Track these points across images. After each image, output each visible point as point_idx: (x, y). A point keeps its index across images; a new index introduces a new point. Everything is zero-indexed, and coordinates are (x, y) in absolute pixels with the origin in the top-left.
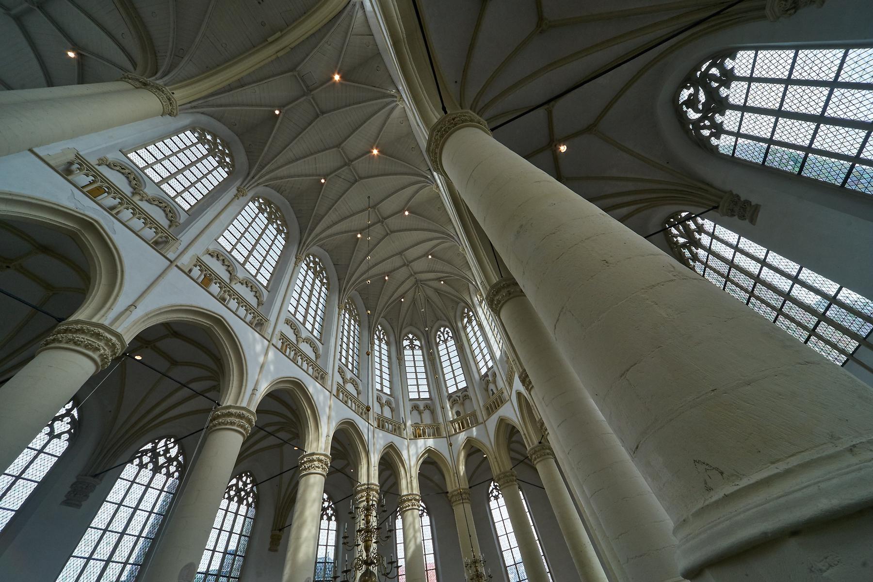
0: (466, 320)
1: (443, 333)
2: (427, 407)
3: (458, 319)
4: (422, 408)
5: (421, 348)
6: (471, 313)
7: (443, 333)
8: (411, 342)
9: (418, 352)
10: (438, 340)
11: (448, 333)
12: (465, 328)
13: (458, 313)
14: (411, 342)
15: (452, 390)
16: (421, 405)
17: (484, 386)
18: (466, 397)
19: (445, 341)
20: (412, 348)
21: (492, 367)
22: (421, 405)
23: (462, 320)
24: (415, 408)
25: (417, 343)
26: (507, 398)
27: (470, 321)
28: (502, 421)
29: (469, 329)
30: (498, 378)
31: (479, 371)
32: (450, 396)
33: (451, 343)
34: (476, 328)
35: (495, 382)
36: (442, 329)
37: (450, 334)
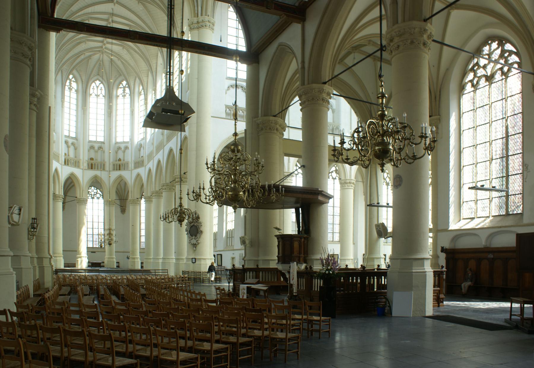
0: (120, 91)
1: (97, 87)
4: (70, 144)
5: (77, 91)
7: (97, 87)
8: (70, 83)
9: (74, 95)
10: (91, 91)
11: (101, 89)
13: (117, 82)
14: (70, 83)
17: (116, 149)
20: (70, 89)
22: (70, 141)
23: (118, 88)
25: (74, 85)
27: (124, 96)
29: (120, 100)
32: (90, 142)
33: (102, 101)
36: (98, 82)
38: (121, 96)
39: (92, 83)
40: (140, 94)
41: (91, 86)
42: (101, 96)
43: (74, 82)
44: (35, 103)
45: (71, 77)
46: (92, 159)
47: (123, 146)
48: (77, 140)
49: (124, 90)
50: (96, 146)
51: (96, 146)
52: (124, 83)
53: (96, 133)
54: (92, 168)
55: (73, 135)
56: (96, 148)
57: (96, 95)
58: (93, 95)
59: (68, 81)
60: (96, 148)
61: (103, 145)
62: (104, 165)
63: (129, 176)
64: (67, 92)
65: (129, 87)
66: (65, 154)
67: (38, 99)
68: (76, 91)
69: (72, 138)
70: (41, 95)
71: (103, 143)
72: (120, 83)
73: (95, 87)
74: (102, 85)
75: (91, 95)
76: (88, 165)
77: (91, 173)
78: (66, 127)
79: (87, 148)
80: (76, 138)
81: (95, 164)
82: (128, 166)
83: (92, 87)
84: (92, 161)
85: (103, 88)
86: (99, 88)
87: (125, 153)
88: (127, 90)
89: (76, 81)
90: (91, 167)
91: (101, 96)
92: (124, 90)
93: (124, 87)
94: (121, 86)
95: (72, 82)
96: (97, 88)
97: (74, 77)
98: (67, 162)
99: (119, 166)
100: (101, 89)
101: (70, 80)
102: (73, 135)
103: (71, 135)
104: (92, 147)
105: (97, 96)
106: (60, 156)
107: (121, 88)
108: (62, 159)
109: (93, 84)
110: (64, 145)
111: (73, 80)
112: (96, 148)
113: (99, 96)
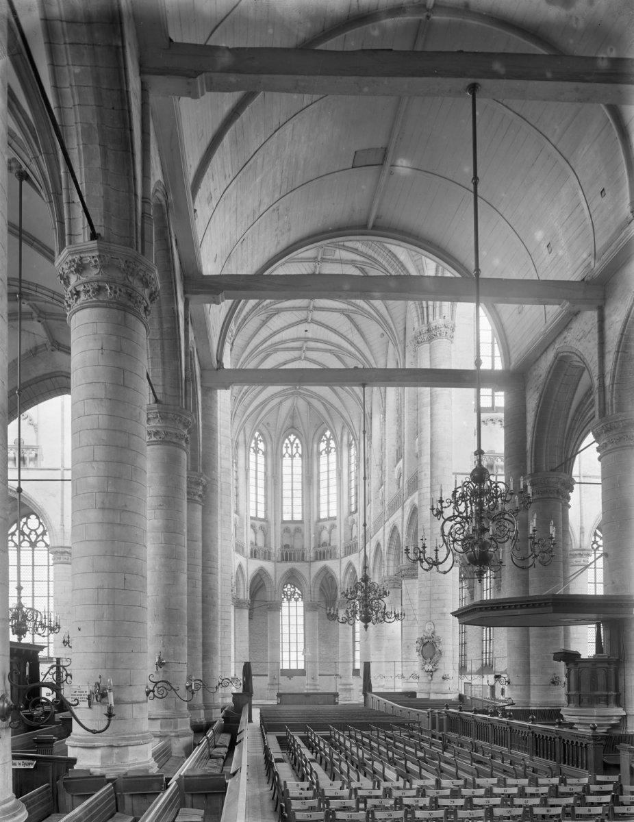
0: (323, 446)
1: (292, 444)
2: (261, 528)
3: (316, 439)
4: (257, 528)
5: (265, 454)
6: (333, 444)
7: (292, 444)
8: (256, 444)
10: (284, 451)
11: (297, 447)
12: (319, 453)
14: (256, 444)
15: (287, 517)
16: (258, 524)
18: (298, 530)
19: (292, 456)
20: (256, 452)
21: (335, 518)
22: (258, 524)
23: (319, 441)
24: (253, 526)
25: (261, 446)
26: (338, 556)
27: (328, 452)
28: (325, 569)
30: (336, 532)
31: (319, 512)
32: (283, 522)
33: (298, 461)
34: (333, 466)
35: (330, 532)
36: (292, 437)
37: (300, 451)
38: (324, 452)
39: (284, 440)
40: (350, 445)
41: (283, 443)
42: (297, 455)
43: (261, 441)
44: (200, 493)
45: (257, 434)
46: (287, 546)
47: (327, 525)
48: (267, 521)
49: (328, 444)
50: (292, 527)
51: (292, 527)
52: (328, 433)
53: (292, 509)
54: (287, 560)
55: (261, 515)
56: (292, 531)
57: (290, 456)
58: (287, 455)
59: (253, 441)
60: (293, 529)
61: (300, 525)
62: (303, 554)
63: (337, 568)
64: (252, 457)
65: (335, 439)
66: (252, 543)
67: (204, 487)
68: (264, 453)
69: (261, 520)
70: (208, 482)
71: (301, 522)
72: (323, 434)
73: (289, 445)
74: (297, 441)
75: (284, 456)
76: (282, 554)
77: (287, 566)
78: (252, 505)
79: (279, 529)
80: (265, 520)
81: (291, 554)
82: (335, 554)
83: (285, 445)
84: (287, 550)
85: (300, 445)
86: (295, 445)
87: (332, 535)
88: (333, 444)
89: (264, 441)
90: (286, 557)
91: (297, 455)
92: (328, 444)
93: (328, 440)
94: (324, 438)
95: (259, 442)
96: (292, 446)
97: (261, 434)
98: (254, 554)
99: (324, 553)
100: (297, 447)
101: (256, 440)
102: (261, 515)
103: (259, 516)
104: (287, 530)
105: (292, 456)
106: (245, 546)
107: (324, 441)
108: (248, 550)
109: (287, 441)
110: (250, 531)
111: (260, 438)
112: (292, 531)
113: (294, 456)
